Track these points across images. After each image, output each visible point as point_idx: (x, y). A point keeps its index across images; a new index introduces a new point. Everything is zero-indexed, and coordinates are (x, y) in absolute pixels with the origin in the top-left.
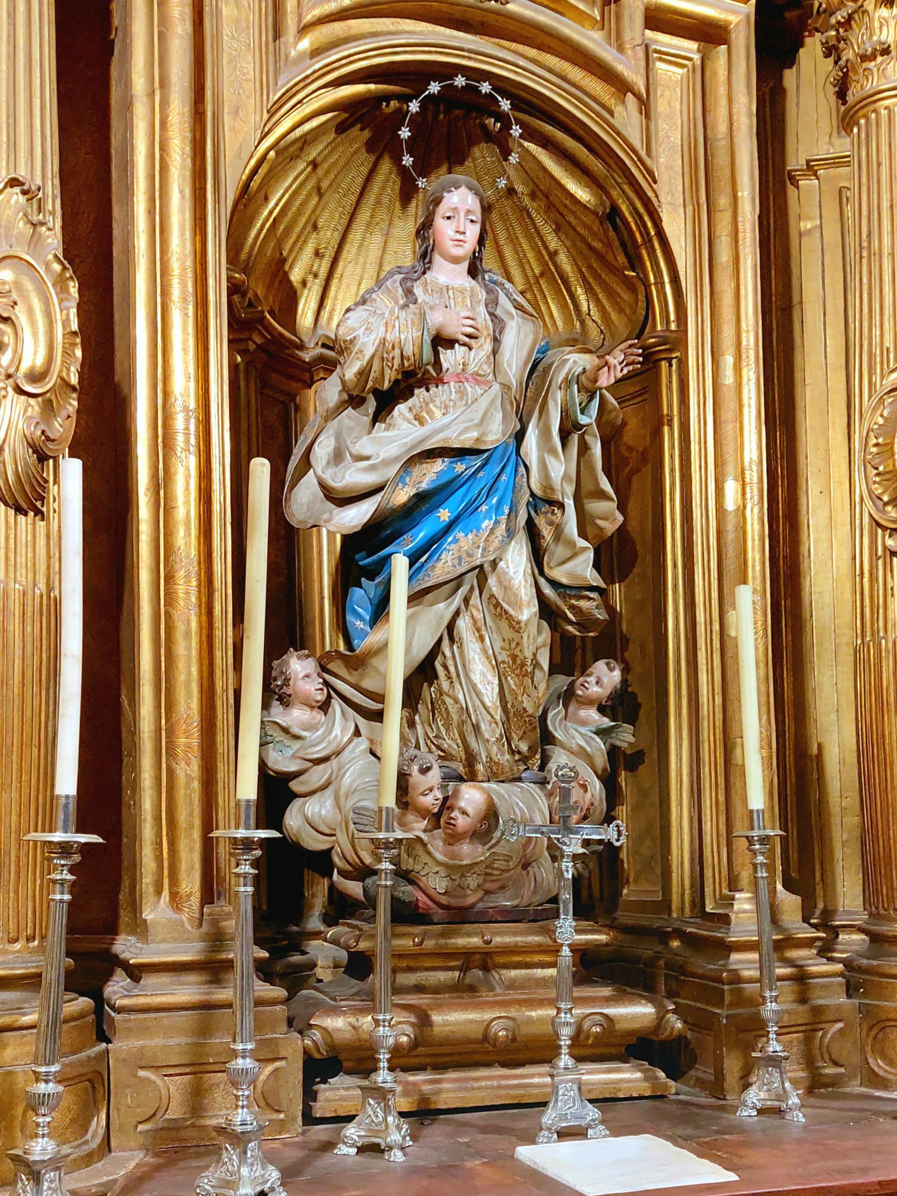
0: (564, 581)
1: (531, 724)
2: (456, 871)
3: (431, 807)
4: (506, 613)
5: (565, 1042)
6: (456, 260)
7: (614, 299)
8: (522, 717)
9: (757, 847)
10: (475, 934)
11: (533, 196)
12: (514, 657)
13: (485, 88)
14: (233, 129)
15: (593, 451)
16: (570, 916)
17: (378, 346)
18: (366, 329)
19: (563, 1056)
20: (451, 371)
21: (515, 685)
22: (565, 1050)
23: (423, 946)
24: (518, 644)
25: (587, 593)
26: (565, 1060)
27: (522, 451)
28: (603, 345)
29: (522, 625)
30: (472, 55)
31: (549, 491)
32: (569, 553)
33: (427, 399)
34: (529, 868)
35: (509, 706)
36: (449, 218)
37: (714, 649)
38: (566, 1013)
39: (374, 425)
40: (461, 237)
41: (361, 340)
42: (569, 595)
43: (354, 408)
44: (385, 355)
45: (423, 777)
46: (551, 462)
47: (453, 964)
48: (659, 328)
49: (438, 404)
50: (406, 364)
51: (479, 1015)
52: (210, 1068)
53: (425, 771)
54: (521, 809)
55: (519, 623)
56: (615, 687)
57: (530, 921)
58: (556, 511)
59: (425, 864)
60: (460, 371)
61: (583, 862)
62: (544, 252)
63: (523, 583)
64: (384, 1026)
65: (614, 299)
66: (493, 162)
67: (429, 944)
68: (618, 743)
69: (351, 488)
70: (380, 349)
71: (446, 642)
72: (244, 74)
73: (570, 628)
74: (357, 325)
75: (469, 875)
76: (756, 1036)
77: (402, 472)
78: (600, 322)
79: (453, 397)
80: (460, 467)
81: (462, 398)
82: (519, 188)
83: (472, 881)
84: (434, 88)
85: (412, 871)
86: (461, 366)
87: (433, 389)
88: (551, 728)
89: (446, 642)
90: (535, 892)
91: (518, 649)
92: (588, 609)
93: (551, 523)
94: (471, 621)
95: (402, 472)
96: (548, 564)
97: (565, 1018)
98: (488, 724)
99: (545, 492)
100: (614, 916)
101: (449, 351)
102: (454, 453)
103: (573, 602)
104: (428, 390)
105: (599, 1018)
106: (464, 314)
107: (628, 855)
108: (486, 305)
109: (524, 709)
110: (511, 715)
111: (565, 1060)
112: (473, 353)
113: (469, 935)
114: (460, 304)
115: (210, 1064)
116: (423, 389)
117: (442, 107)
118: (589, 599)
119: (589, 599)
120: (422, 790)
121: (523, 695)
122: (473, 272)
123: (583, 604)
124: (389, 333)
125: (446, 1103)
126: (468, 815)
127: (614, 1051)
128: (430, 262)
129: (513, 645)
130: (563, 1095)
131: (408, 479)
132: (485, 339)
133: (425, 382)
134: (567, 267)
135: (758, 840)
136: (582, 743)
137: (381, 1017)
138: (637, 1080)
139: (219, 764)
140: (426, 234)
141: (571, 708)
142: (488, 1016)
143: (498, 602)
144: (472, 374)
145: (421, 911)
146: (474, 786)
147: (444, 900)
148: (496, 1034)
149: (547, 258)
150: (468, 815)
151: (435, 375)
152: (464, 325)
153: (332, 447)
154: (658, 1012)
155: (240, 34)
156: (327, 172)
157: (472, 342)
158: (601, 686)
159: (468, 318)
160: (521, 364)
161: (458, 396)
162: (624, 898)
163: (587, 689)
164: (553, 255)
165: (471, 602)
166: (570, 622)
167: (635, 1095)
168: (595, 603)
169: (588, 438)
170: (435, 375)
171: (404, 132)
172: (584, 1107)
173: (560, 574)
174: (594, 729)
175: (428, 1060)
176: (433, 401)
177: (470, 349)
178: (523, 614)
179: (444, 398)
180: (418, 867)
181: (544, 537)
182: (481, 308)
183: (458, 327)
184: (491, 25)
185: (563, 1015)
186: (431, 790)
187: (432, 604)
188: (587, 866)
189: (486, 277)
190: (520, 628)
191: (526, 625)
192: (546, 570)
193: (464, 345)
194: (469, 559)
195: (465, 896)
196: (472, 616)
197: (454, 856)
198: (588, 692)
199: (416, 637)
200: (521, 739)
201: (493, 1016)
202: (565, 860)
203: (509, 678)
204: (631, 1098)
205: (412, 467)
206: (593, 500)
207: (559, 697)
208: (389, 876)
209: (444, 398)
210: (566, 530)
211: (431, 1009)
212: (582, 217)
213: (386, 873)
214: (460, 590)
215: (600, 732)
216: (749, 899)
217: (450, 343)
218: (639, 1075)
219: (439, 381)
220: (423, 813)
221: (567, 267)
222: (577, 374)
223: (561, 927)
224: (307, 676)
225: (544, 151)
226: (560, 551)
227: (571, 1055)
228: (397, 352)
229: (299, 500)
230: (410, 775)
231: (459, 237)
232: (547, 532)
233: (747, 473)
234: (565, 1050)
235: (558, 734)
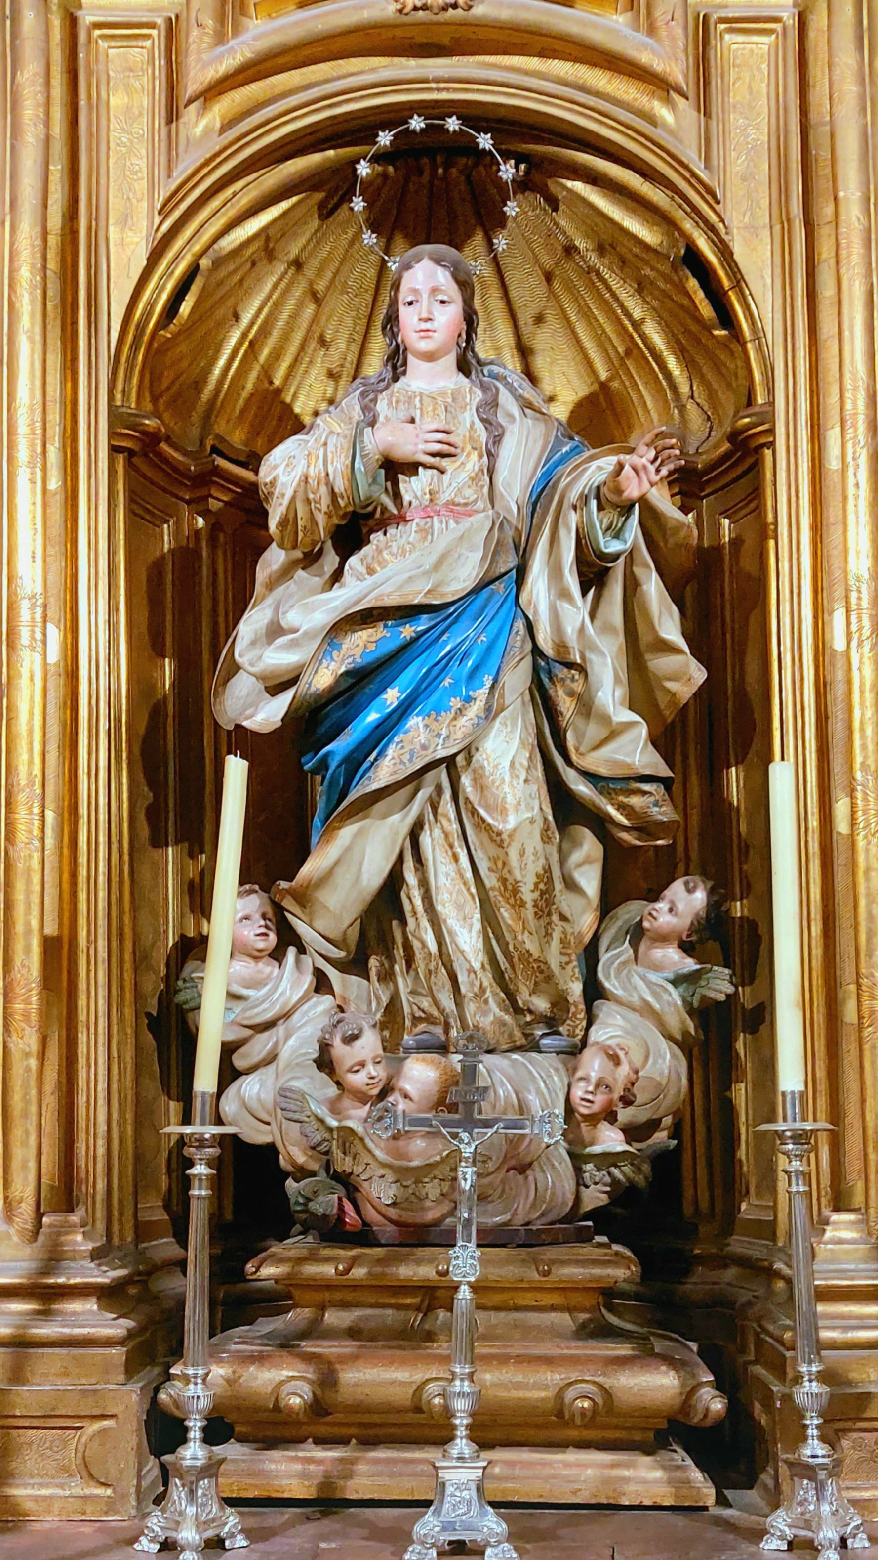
0: (604, 771)
1: (542, 972)
2: (402, 1174)
3: (365, 1089)
4: (484, 821)
5: (461, 1421)
6: (430, 357)
7: (718, 368)
8: (529, 963)
9: (790, 1147)
10: (430, 1261)
11: (601, 250)
12: (504, 881)
13: (453, 124)
14: (122, 243)
15: (645, 587)
16: (472, 1245)
17: (299, 485)
18: (287, 465)
19: (458, 1441)
20: (414, 504)
21: (513, 920)
22: (461, 1432)
23: (350, 1276)
24: (504, 864)
25: (639, 785)
26: (462, 1445)
27: (523, 599)
28: (709, 436)
29: (505, 836)
30: (442, 85)
31: (562, 650)
32: (604, 733)
33: (382, 545)
34: (529, 1172)
35: (511, 948)
36: (410, 303)
37: (811, 855)
38: (462, 1380)
39: (333, 585)
40: (428, 326)
41: (282, 477)
42: (614, 790)
43: (303, 569)
44: (311, 496)
45: (347, 1048)
46: (564, 607)
47: (408, 1301)
48: (760, 401)
49: (394, 550)
50: (342, 503)
51: (407, 1374)
52: (22, 1422)
53: (351, 1039)
54: (506, 1091)
55: (499, 834)
56: (697, 915)
57: (519, 1246)
58: (577, 677)
59: (367, 1164)
60: (427, 503)
61: (632, 1164)
62: (626, 322)
63: (507, 779)
64: (196, 1384)
65: (718, 368)
66: (537, 216)
67: (359, 1273)
68: (712, 994)
69: (271, 672)
70: (301, 490)
71: (409, 864)
72: (136, 173)
73: (625, 836)
74: (278, 462)
75: (426, 1180)
76: (837, 1431)
77: (325, 646)
78: (706, 408)
79: (411, 539)
80: (408, 631)
81: (425, 539)
82: (581, 243)
83: (432, 1189)
84: (385, 139)
85: (352, 1173)
86: (428, 496)
87: (391, 531)
88: (600, 974)
89: (409, 864)
90: (534, 1205)
91: (505, 871)
92: (642, 807)
93: (571, 694)
94: (443, 836)
95: (325, 646)
96: (577, 750)
97: (462, 1386)
98: (466, 973)
99: (558, 652)
100: (727, 1241)
101: (414, 478)
102: (400, 614)
103: (621, 798)
104: (385, 534)
105: (591, 1387)
106: (434, 426)
107: (747, 1154)
108: (477, 410)
109: (528, 951)
110: (516, 960)
111: (462, 1445)
112: (446, 477)
113: (419, 1262)
114: (431, 414)
115: (15, 1417)
116: (380, 533)
117: (439, 159)
118: (644, 793)
119: (644, 793)
120: (348, 1064)
121: (523, 933)
122: (463, 368)
123: (635, 801)
124: (312, 466)
125: (357, 1492)
126: (411, 1099)
127: (637, 1436)
128: (405, 364)
129: (500, 865)
130: (452, 1495)
131: (335, 653)
132: (468, 455)
133: (384, 522)
134: (658, 340)
135: (791, 1138)
136: (649, 998)
137: (190, 1371)
138: (656, 1481)
139: (80, 1035)
140: (395, 330)
141: (642, 948)
142: (419, 1376)
143: (473, 807)
144: (447, 504)
145: (348, 1228)
146: (424, 1060)
147: (392, 1213)
148: (429, 1402)
149: (631, 329)
150: (411, 1099)
151: (395, 512)
152: (426, 442)
153: (266, 621)
154: (683, 1385)
155: (131, 125)
156: (320, 272)
157: (445, 463)
158: (676, 915)
159: (437, 431)
160: (525, 481)
161: (418, 536)
162: (742, 1216)
163: (655, 919)
164: (637, 325)
165: (440, 810)
166: (625, 828)
167: (647, 1502)
168: (652, 799)
169: (638, 571)
170: (395, 512)
171: (357, 203)
172: (484, 1514)
173: (596, 762)
174: (671, 976)
175: (353, 1431)
176: (388, 547)
177: (442, 472)
178: (505, 822)
179: (404, 540)
180: (358, 1169)
181: (562, 714)
182: (467, 415)
183: (416, 445)
184: (469, 39)
185: (457, 1382)
186: (363, 1064)
187: (384, 816)
188: (639, 1169)
189: (486, 372)
190: (502, 841)
191: (510, 836)
192: (574, 757)
193: (431, 467)
194: (424, 753)
195: (423, 1209)
196: (442, 828)
197: (400, 1155)
198: (656, 924)
199: (366, 861)
200: (533, 992)
201: (427, 1376)
202: (463, 1164)
203: (502, 910)
204: (640, 1507)
205: (341, 637)
206: (659, 655)
207: (627, 933)
208: (204, 1184)
209: (404, 540)
210: (596, 701)
211: (341, 1362)
212: (659, 266)
213: (200, 1180)
214: (420, 794)
215: (676, 982)
216: (853, 1223)
217: (412, 468)
218: (658, 1474)
219: (401, 519)
220: (362, 1098)
221: (658, 340)
222: (596, 484)
223: (457, 1258)
224: (247, 918)
225: (595, 188)
226: (594, 731)
227: (472, 1438)
228: (323, 490)
229: (237, 693)
230: (332, 1046)
231: (424, 326)
232: (566, 706)
233: (854, 596)
234: (461, 1432)
235: (610, 984)
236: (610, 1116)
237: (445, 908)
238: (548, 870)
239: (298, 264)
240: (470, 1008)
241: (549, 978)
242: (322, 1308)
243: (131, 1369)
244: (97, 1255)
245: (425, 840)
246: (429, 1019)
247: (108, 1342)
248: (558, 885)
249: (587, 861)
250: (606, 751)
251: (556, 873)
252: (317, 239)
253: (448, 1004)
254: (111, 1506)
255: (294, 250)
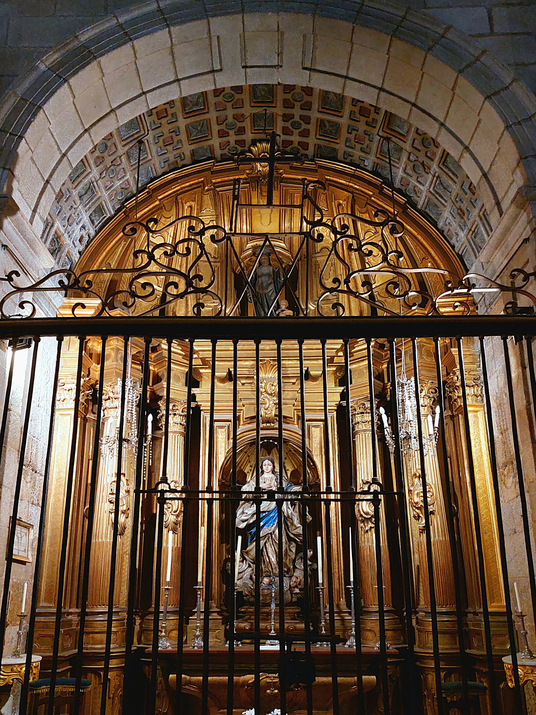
71: (264, 548)
83: (268, 598)
89: (264, 548)
142: (266, 625)
173: (294, 532)
226: (294, 528)
236: (297, 587)
237: (270, 555)
238: (286, 549)
239: (246, 452)
240: (274, 570)
241: (287, 565)
242: (251, 616)
243: (223, 624)
244: (216, 607)
245: (267, 545)
246: (267, 572)
247: (219, 619)
248: (288, 551)
249: (293, 547)
250: (296, 531)
251: (288, 549)
252: (249, 449)
253: (270, 569)
254: (220, 642)
255: (245, 451)
